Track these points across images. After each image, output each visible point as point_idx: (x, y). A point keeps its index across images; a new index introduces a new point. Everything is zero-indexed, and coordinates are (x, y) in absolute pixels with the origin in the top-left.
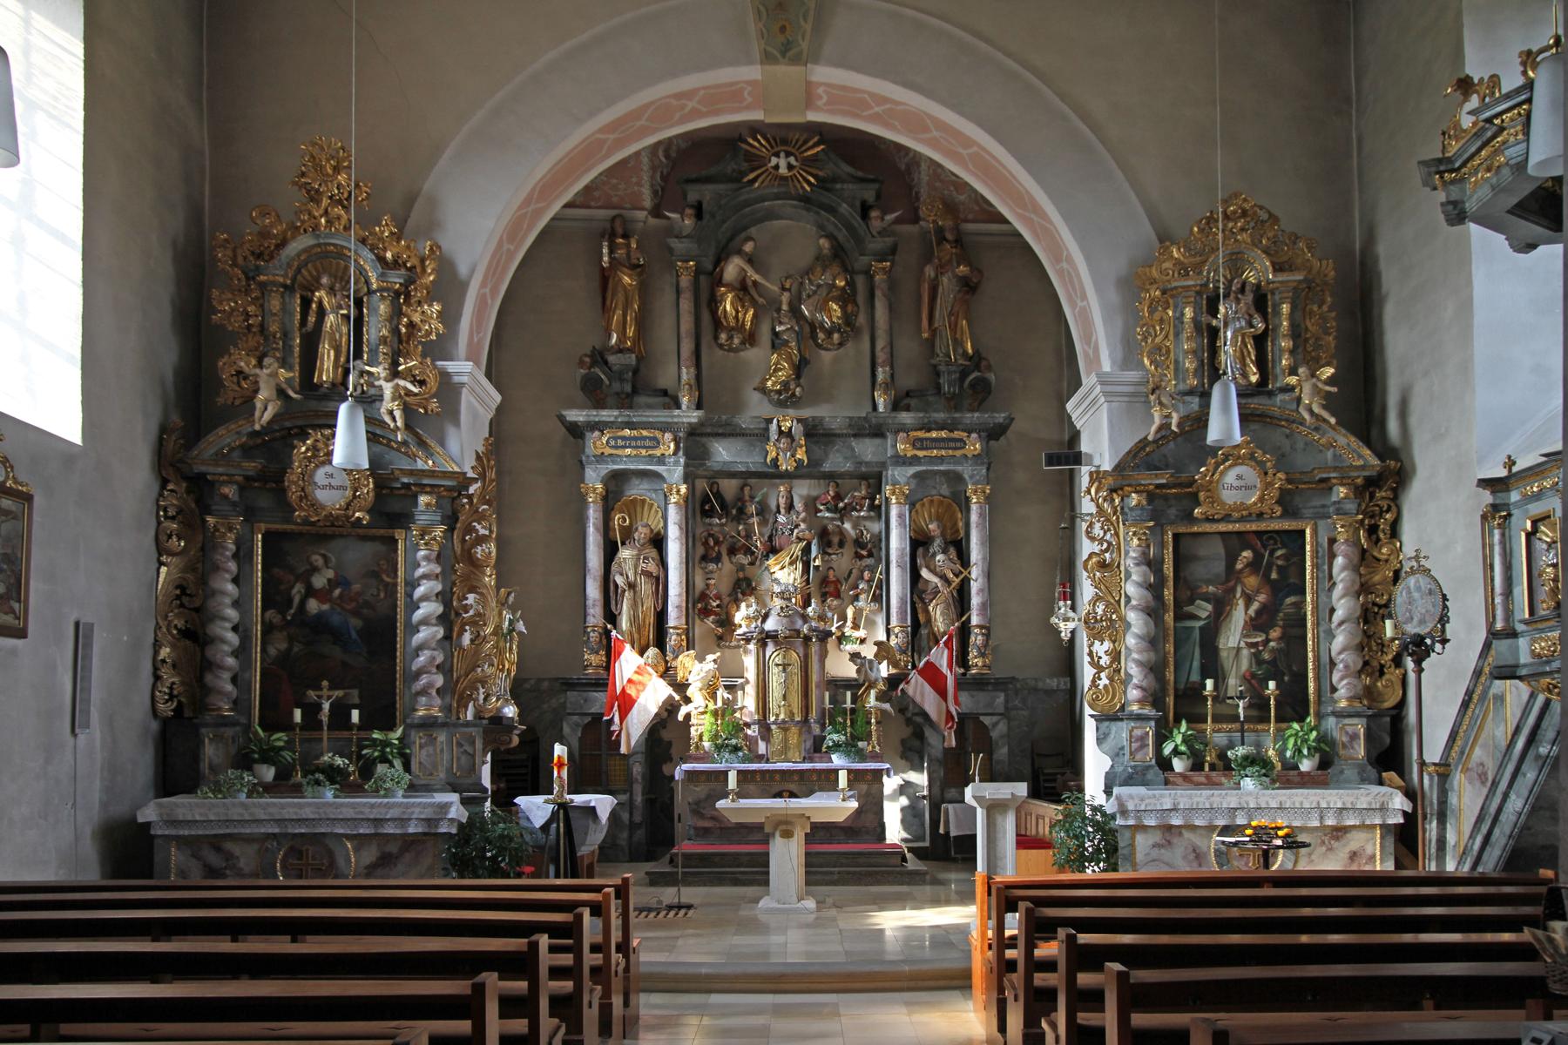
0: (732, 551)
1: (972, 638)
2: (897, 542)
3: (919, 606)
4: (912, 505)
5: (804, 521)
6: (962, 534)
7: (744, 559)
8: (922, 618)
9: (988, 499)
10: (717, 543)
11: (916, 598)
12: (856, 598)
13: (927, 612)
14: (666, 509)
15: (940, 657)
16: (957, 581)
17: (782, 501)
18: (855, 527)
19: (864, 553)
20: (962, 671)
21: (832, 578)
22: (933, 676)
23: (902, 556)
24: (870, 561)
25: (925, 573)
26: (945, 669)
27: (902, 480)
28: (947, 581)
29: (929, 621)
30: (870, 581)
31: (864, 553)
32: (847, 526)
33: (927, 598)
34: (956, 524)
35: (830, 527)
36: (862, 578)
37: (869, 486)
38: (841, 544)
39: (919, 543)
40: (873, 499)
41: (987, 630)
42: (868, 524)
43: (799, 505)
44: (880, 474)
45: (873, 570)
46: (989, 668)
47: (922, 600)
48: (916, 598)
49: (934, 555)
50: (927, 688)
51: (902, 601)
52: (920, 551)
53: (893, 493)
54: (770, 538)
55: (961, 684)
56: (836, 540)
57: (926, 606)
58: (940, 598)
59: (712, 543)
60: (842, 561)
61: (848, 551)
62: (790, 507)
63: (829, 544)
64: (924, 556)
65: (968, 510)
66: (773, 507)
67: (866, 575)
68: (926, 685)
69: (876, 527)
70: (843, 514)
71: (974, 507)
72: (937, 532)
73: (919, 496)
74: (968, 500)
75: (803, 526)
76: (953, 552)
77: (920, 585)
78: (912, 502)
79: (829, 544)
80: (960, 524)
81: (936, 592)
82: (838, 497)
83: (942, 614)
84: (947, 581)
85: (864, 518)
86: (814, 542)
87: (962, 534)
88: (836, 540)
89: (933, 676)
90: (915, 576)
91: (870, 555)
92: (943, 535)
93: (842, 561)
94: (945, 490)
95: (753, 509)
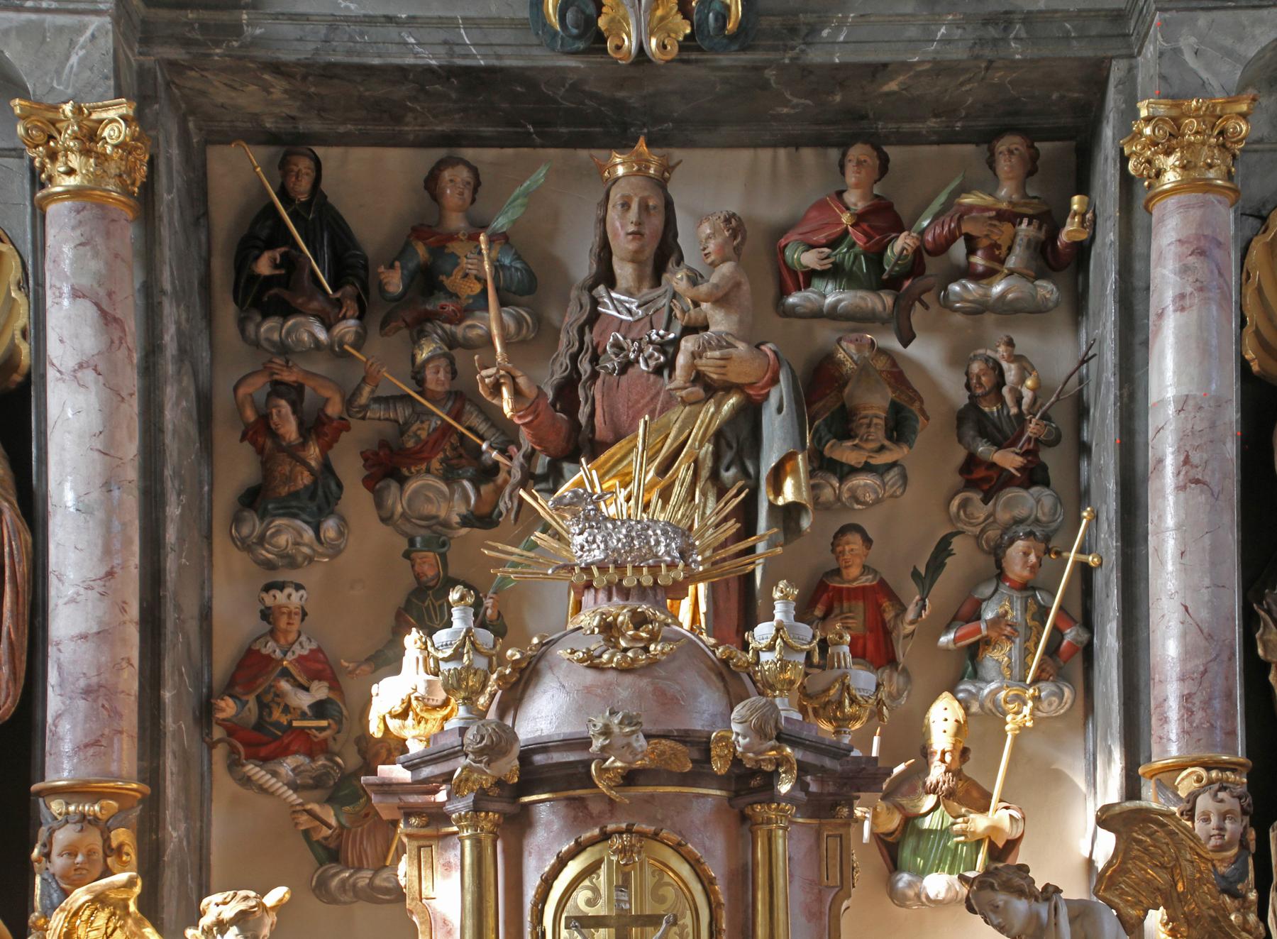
0: (387, 466)
5: (722, 300)
7: (445, 500)
10: (316, 426)
12: (969, 661)
14: (39, 246)
17: (621, 227)
18: (959, 358)
21: (854, 576)
32: (926, 353)
35: (848, 354)
38: (899, 426)
43: (698, 237)
44: (1096, 78)
53: (1171, 140)
54: (567, 391)
56: (874, 403)
59: (290, 429)
60: (899, 505)
61: (932, 457)
62: (663, 255)
63: (844, 424)
66: (583, 267)
69: (1054, 355)
70: (906, 285)
75: (720, 322)
79: (844, 424)
82: (883, 218)
85: (1006, 310)
86: (780, 393)
88: (874, 403)
91: (1034, 475)
93: (899, 505)
95: (482, 260)
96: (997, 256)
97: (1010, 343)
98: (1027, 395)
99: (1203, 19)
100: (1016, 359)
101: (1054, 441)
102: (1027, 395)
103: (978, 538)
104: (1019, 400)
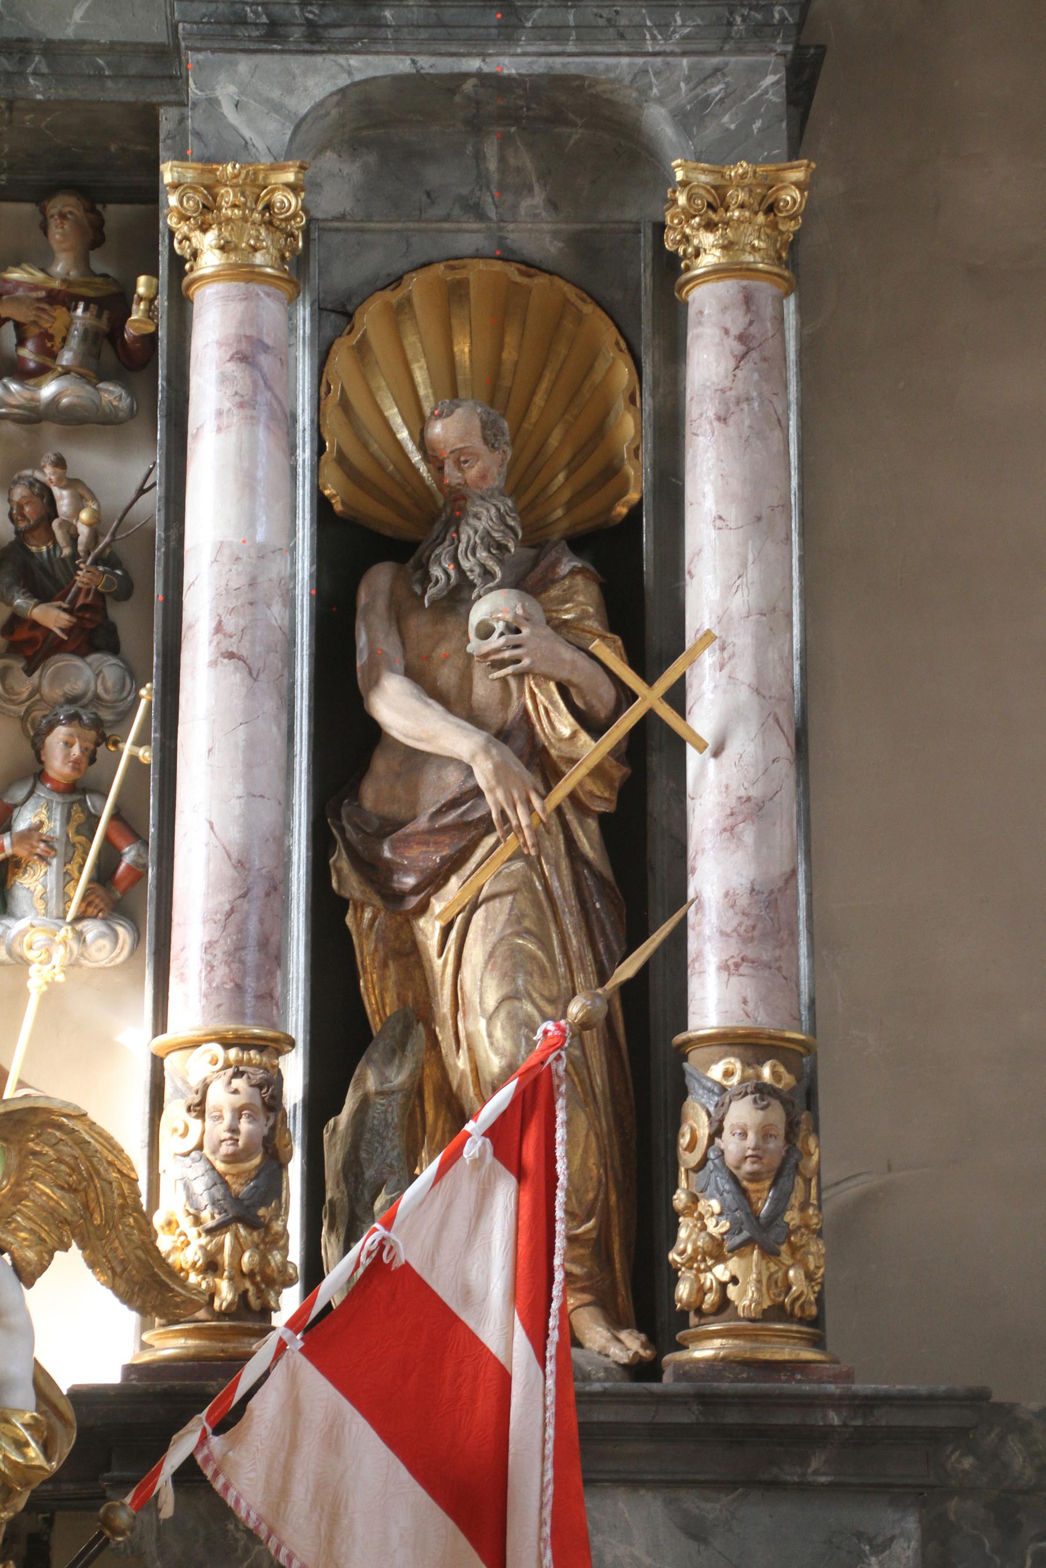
1: (697, 1121)
2: (232, 517)
3: (363, 922)
4: (337, 315)
6: (638, 483)
8: (378, 995)
9: (797, 263)
11: (347, 880)
13: (408, 955)
15: (466, 1236)
16: (593, 751)
19: (52, 617)
20: (631, 1345)
22: (396, 1353)
23: (251, 593)
24: (87, 674)
25: (398, 708)
26: (494, 1322)
27: (265, 134)
28: (542, 764)
29: (418, 1013)
30: (79, 790)
31: (52, 617)
33: (409, 863)
34: (600, 431)
36: (40, 775)
37: (94, 237)
39: (369, 546)
40: (116, 303)
41: (796, 1077)
42: (92, 461)
45: (103, 734)
46: (815, 1327)
47: (377, 874)
48: (347, 880)
49: (459, 596)
50: (371, 1463)
51: (255, 886)
52: (378, 582)
55: (599, 1438)
57: (401, 909)
58: (489, 867)
64: (398, 617)
65: (675, 352)
67: (61, 751)
68: (359, 1430)
71: (710, 313)
72: (485, 468)
73: (373, 261)
74: (670, 268)
76: (580, 600)
77: (373, 794)
78: (333, 289)
80: (628, 427)
81: (467, 827)
83: (509, 961)
84: (542, 764)
87: (638, 483)
89: (396, 1353)
90: (346, 743)
92: (522, 483)
94: (535, 225)
96: (49, 353)
97: (60, 463)
98: (83, 531)
99: (244, 64)
100: (72, 484)
101: (125, 591)
102: (83, 531)
103: (23, 719)
104: (73, 538)
